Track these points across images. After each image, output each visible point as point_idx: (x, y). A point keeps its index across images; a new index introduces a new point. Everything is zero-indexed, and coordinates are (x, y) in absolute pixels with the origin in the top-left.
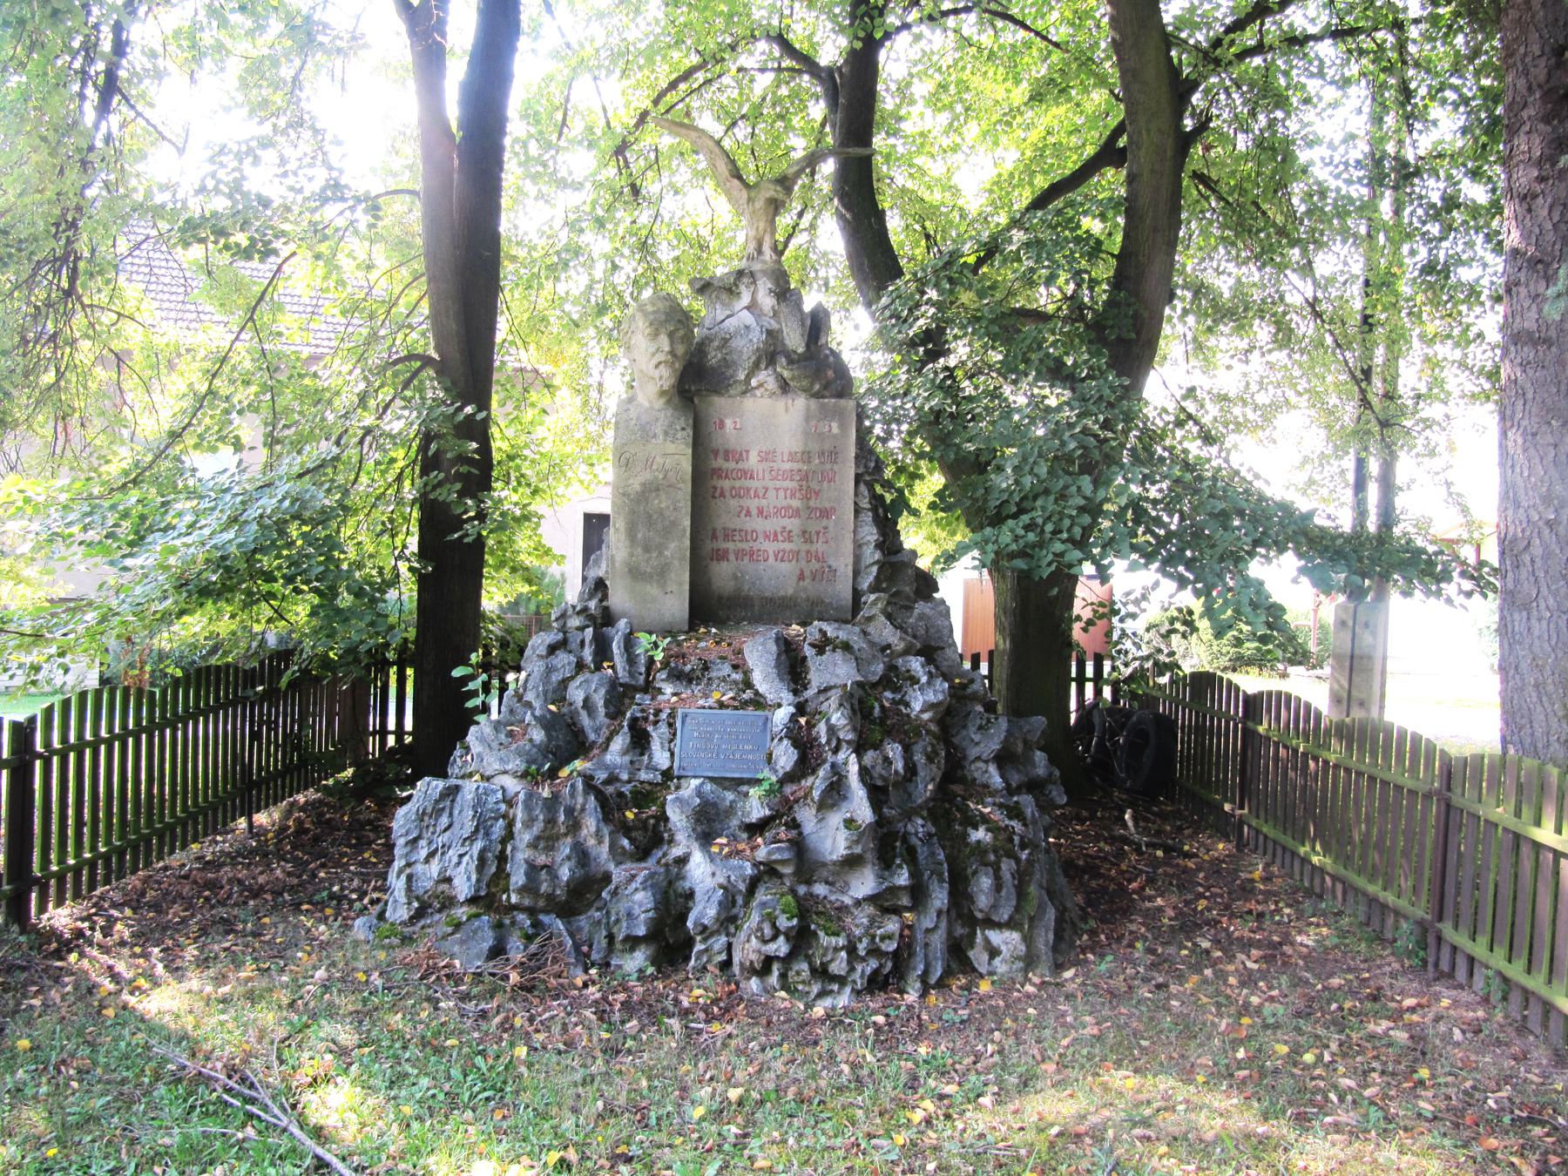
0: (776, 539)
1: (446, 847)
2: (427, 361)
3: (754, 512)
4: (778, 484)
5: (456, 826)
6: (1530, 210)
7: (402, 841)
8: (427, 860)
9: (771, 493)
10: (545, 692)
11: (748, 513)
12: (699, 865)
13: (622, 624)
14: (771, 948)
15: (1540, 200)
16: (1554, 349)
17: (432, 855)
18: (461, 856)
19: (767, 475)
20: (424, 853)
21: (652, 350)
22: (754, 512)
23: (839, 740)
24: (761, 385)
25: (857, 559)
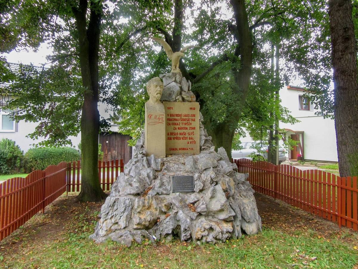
0: (182, 135)
1: (116, 215)
2: (231, 27)
3: (177, 128)
4: (183, 122)
5: (119, 209)
6: (340, 61)
7: (103, 214)
8: (111, 218)
9: (181, 124)
10: (245, 179)
11: (176, 129)
12: (181, 214)
13: (152, 156)
14: (204, 234)
15: (342, 59)
16: (347, 90)
17: (112, 217)
18: (121, 217)
19: (180, 120)
20: (110, 217)
21: (155, 91)
22: (177, 128)
23: (213, 181)
24: (178, 99)
25: (200, 138)
